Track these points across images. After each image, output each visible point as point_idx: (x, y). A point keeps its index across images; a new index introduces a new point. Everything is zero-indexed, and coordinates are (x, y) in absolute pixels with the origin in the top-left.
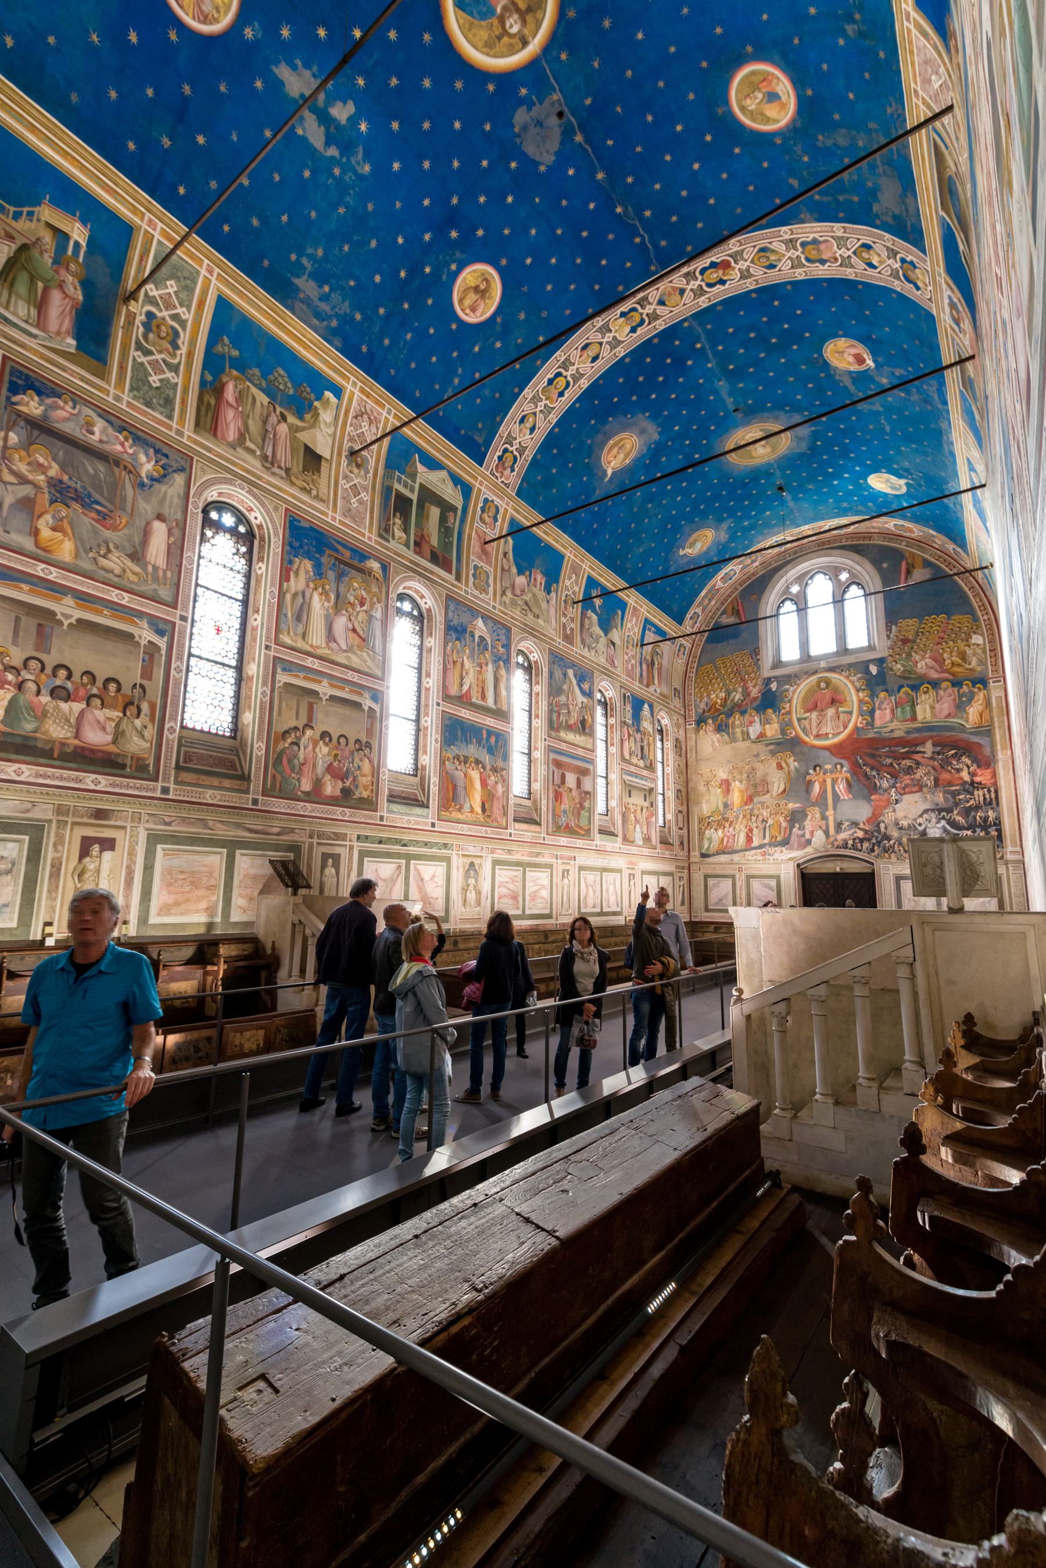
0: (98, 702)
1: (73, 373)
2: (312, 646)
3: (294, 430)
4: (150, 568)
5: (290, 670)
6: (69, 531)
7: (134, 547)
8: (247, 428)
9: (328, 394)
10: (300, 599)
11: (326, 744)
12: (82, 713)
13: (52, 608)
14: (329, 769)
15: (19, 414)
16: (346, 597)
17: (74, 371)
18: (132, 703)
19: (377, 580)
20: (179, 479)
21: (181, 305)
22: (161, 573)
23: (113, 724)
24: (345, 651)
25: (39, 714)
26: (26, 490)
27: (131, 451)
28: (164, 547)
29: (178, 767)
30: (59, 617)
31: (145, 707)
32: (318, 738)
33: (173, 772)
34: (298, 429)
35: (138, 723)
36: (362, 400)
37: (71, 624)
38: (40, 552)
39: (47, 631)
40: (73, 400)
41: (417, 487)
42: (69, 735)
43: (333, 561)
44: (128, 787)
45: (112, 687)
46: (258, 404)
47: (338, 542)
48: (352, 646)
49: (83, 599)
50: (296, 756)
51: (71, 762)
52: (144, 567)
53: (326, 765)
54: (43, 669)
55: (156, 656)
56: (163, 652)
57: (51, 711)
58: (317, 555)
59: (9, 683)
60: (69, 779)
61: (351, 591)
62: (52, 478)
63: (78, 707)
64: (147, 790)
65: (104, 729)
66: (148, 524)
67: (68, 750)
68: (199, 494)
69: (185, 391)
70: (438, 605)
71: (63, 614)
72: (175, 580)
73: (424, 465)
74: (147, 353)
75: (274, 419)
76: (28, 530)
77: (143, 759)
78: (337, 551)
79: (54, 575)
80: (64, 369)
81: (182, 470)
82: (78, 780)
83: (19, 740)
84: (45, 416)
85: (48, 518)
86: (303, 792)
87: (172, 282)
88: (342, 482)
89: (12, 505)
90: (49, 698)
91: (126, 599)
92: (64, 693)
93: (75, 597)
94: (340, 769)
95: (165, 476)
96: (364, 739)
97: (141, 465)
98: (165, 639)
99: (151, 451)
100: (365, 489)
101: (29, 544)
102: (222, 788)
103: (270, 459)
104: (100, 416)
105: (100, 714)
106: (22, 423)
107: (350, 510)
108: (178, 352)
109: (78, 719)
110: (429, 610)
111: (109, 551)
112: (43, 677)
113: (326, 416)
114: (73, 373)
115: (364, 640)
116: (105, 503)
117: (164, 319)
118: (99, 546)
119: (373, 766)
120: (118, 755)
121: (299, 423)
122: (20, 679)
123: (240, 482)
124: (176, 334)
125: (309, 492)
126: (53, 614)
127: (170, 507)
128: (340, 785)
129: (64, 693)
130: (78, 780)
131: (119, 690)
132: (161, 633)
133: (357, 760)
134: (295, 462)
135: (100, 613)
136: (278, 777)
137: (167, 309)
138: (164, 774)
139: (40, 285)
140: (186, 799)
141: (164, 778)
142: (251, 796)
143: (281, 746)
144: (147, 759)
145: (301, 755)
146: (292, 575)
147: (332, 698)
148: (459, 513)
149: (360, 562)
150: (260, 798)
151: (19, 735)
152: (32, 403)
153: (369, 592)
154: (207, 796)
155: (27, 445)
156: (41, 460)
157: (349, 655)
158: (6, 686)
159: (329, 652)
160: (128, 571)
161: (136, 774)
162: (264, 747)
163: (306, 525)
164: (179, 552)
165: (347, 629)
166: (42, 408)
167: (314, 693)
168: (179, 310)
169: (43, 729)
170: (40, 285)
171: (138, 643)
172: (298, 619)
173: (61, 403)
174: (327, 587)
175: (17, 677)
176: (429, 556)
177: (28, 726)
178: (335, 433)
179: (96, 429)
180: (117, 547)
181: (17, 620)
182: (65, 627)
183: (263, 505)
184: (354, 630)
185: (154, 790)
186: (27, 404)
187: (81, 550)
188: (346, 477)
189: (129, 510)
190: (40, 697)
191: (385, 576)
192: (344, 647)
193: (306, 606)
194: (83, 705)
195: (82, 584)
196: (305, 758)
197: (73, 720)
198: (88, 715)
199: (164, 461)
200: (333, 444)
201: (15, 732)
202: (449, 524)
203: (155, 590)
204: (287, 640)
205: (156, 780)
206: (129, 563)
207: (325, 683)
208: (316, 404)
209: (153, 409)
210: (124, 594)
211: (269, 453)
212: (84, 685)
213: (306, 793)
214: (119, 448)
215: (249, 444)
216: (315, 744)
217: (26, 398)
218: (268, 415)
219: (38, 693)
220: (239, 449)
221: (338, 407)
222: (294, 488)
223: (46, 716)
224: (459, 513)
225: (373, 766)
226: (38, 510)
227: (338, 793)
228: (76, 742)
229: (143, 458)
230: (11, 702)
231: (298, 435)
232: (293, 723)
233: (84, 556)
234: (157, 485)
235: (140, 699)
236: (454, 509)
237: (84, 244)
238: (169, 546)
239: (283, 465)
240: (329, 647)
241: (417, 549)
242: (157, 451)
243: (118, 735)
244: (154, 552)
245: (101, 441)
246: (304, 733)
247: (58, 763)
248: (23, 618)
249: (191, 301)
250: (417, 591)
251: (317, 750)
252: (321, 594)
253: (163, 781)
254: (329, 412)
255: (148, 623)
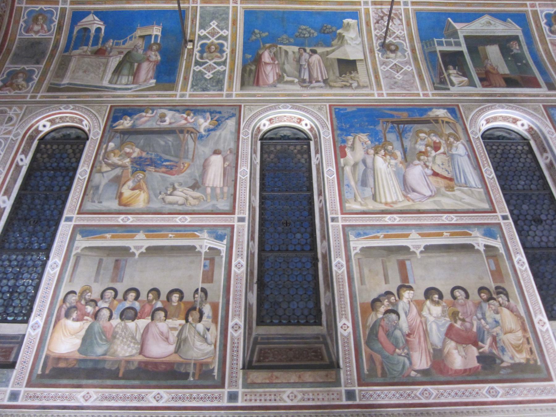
0: (162, 314)
1: (152, 96)
2: (386, 204)
3: (323, 56)
4: (209, 190)
5: (365, 234)
6: (145, 187)
7: (195, 179)
8: (284, 71)
9: (346, 21)
10: (362, 167)
11: (437, 303)
12: (147, 328)
13: (127, 245)
14: (450, 333)
15: (117, 131)
16: (415, 148)
17: (153, 95)
18: (194, 309)
19: (448, 123)
20: (231, 123)
21: (222, 29)
22: (218, 191)
23: (176, 333)
24: (430, 196)
25: (110, 337)
26: (118, 171)
27: (193, 120)
28: (220, 171)
29: (248, 366)
30: (133, 250)
31: (207, 310)
32: (422, 297)
33: (241, 373)
34: (328, 53)
35: (200, 327)
36: (377, 9)
37: (142, 254)
38: (122, 208)
39: (122, 263)
40: (151, 109)
41: (462, 40)
42: (134, 351)
43: (390, 125)
44: (191, 398)
45: (175, 297)
46: (290, 53)
47: (391, 110)
48: (438, 189)
49: (151, 231)
50: (396, 326)
51: (134, 379)
52: (204, 192)
53: (444, 330)
54: (115, 297)
55: (217, 259)
56: (223, 254)
57: (120, 332)
58: (372, 127)
59: (88, 315)
60: (132, 398)
61: (419, 142)
62: (135, 158)
63: (142, 323)
64: (212, 399)
65: (167, 339)
66: (206, 160)
67: (133, 368)
68: (248, 125)
69: (232, 70)
70: (537, 118)
71: (136, 247)
72: (232, 191)
73: (461, 22)
74: (201, 64)
75: (306, 56)
76: (115, 196)
77: (207, 364)
78: (392, 116)
79: (131, 220)
80: (147, 96)
81: (234, 115)
82: (141, 398)
83: (90, 365)
84: (133, 126)
85: (130, 184)
86: (417, 371)
87: (214, 21)
88: (380, 68)
89: (107, 185)
90: (119, 320)
91: (188, 220)
92: (131, 313)
93: (145, 231)
94: (470, 330)
95: (219, 125)
96: (492, 285)
97: (200, 125)
98: (225, 242)
99: (208, 115)
100: (408, 63)
101: (114, 205)
102: (303, 384)
103: (308, 80)
104: (170, 110)
105: (163, 326)
106: (118, 135)
107: (396, 83)
108: (225, 54)
109: (142, 335)
110: (530, 130)
111: (174, 189)
112: (115, 302)
113: (351, 35)
114: (152, 96)
115: (451, 179)
116: (172, 159)
117: (212, 43)
118: (167, 189)
119: (518, 316)
120: (180, 364)
121: (329, 49)
122: (97, 308)
123: (283, 104)
124: (222, 45)
125: (350, 86)
126: (127, 249)
127: (224, 142)
128: (474, 352)
129: (131, 313)
130: (141, 398)
131: (181, 298)
132: (220, 238)
133: (490, 314)
134: (331, 73)
135: (165, 237)
136: (378, 357)
137: (213, 36)
138: (231, 377)
139: (136, 64)
140: (258, 404)
141: (231, 382)
142: (343, 389)
143: (372, 318)
144: (211, 363)
145: (404, 323)
146: (348, 151)
147: (428, 248)
148: (522, 38)
149: (422, 115)
150: (357, 388)
151: (91, 360)
152: (125, 122)
153: (440, 135)
154: (285, 396)
155: (120, 147)
156: (128, 150)
157: (436, 199)
158: (86, 318)
159: (410, 203)
160: (190, 198)
161: (199, 383)
162: (350, 324)
163: (354, 109)
164: (234, 170)
165: (426, 176)
166: (132, 122)
167: (405, 249)
168: (222, 33)
169: (112, 350)
170: (136, 64)
171: (200, 252)
172: (364, 183)
173: (144, 114)
174: (390, 147)
175: (94, 308)
176: (503, 82)
177: (99, 350)
178: (363, 41)
179: (168, 119)
180: (181, 185)
181: (100, 262)
182: (137, 257)
183: (307, 111)
184: (435, 174)
185: (220, 398)
186: (123, 124)
187: (152, 196)
188: (384, 63)
189: (190, 156)
190: (112, 321)
191: (455, 117)
192: (428, 193)
193: (370, 173)
194: (148, 320)
195: (152, 220)
196: (410, 327)
197: (138, 337)
198: (153, 330)
199: (218, 116)
200: (364, 47)
201: (88, 358)
202: (515, 51)
203: (214, 205)
204: (356, 207)
205: (222, 386)
206: (191, 192)
207: (414, 234)
208: (339, 31)
209: (208, 90)
210: (186, 216)
211: (306, 77)
212: (149, 302)
213: (424, 372)
214: (184, 122)
215: (287, 78)
216: (420, 305)
217: (122, 121)
218: (301, 55)
219: (110, 317)
220: (279, 85)
221: (359, 25)
222: (334, 89)
223: (114, 337)
224: (522, 38)
225: (518, 316)
226: (123, 180)
227: (474, 363)
228: (141, 358)
229: (201, 120)
230: (87, 331)
231: (332, 56)
232: (383, 288)
233: (155, 199)
234: (213, 133)
235: (201, 304)
236: (516, 38)
237: (159, 34)
238: (225, 169)
239: (320, 79)
240: (408, 199)
241: (486, 83)
242: (211, 113)
243: (181, 342)
244: (213, 176)
245: (170, 123)
246: (400, 296)
247: (122, 382)
248: (105, 259)
249: (228, 24)
250: (505, 119)
251: (425, 313)
252: (385, 155)
253: (230, 386)
254: (352, 30)
255: (208, 232)
